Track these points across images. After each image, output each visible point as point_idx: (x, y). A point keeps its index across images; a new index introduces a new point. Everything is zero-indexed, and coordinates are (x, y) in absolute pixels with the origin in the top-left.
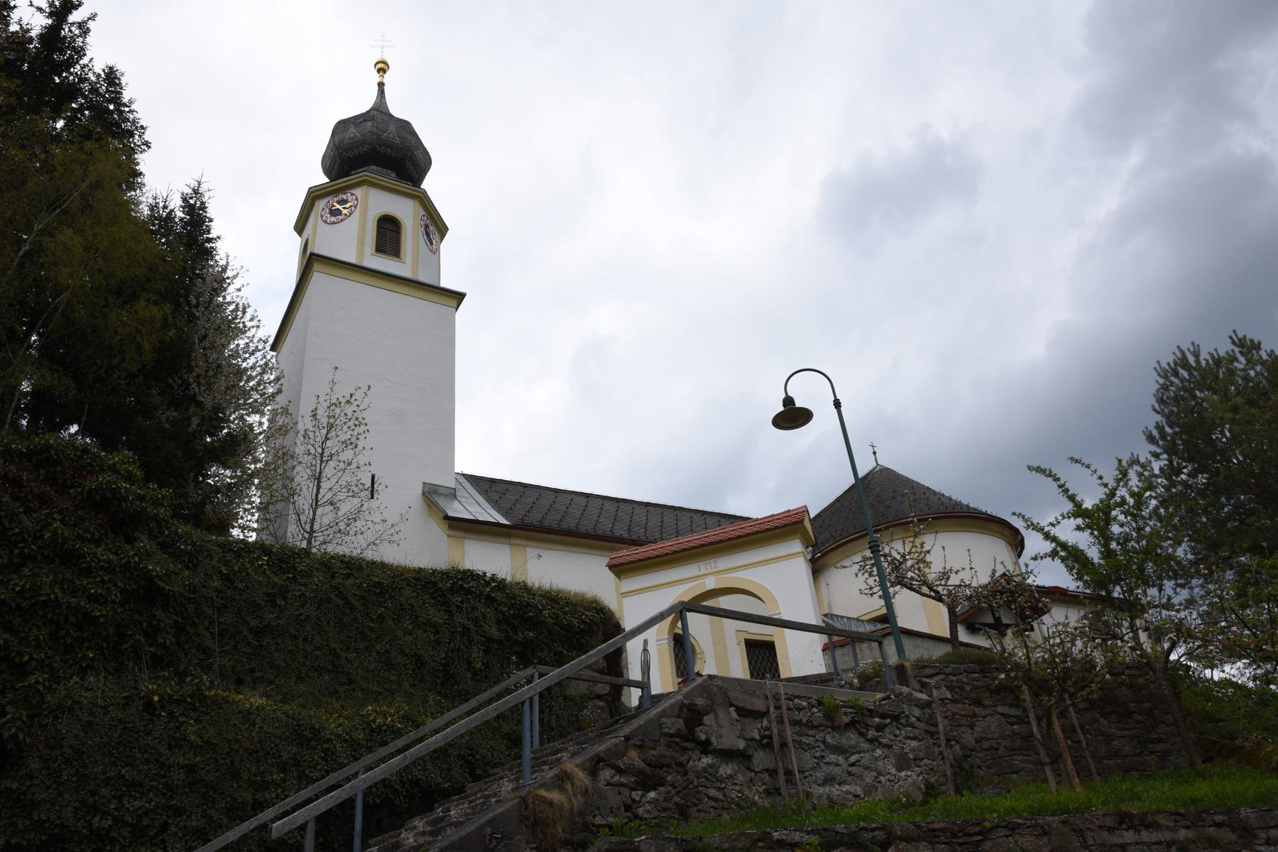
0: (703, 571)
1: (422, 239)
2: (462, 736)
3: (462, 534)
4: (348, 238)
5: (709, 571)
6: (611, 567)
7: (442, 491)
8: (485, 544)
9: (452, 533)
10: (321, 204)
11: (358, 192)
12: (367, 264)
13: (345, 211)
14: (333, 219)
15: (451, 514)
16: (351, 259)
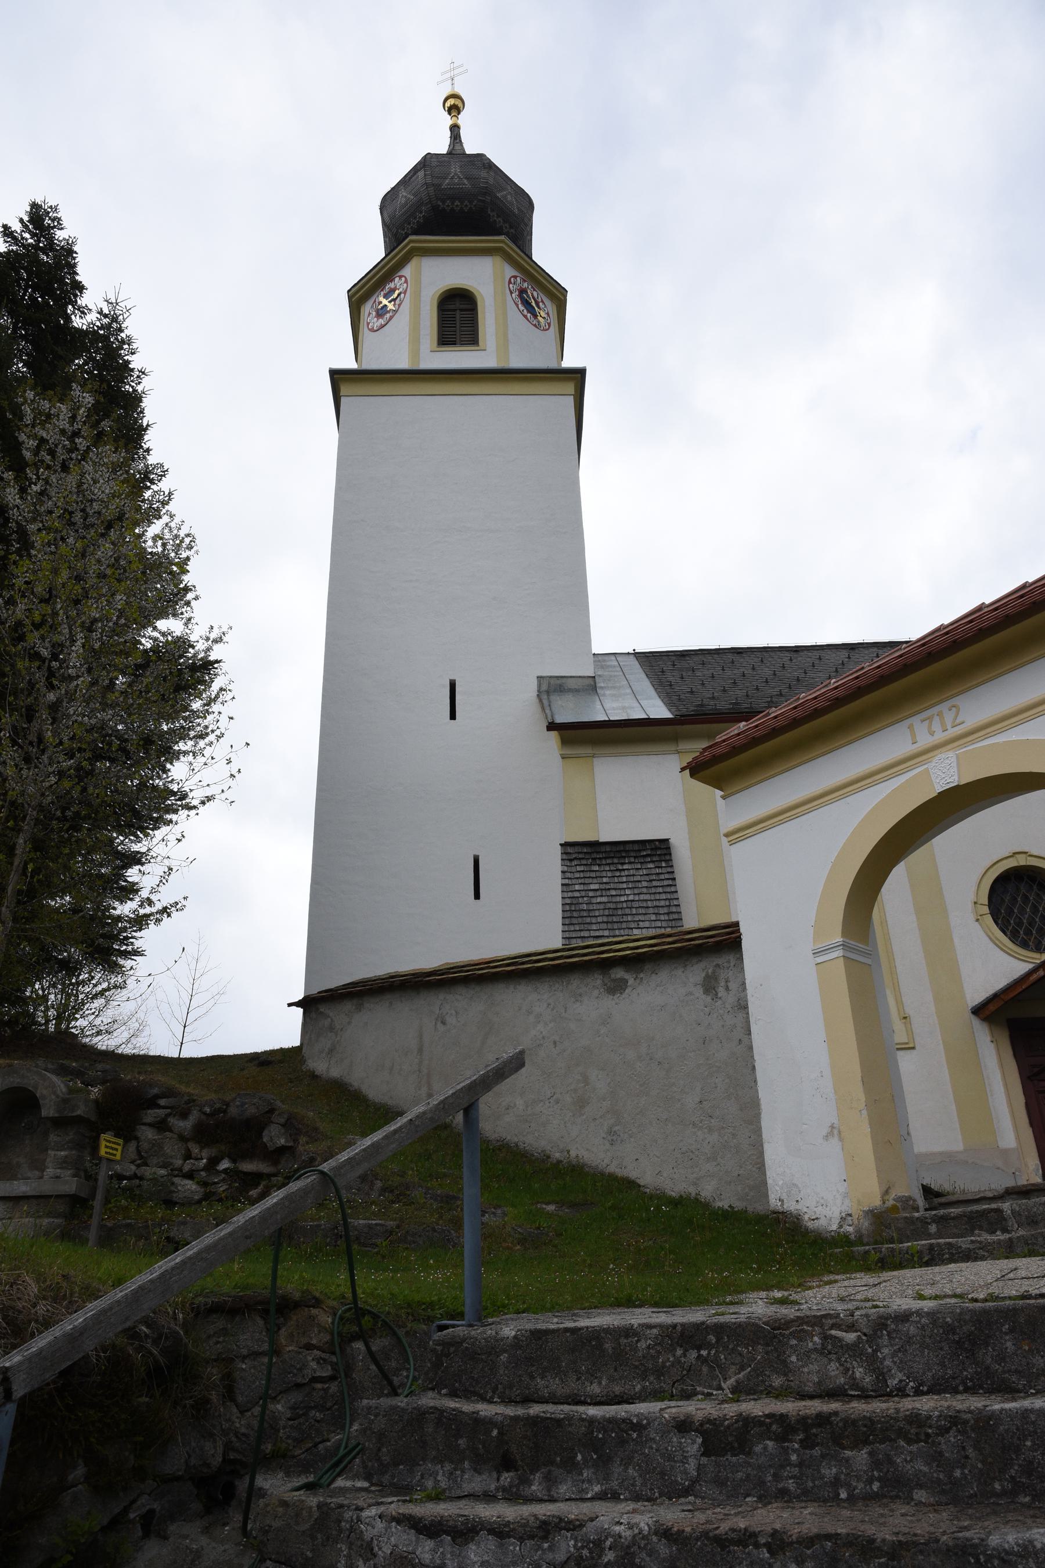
0: (925, 740)
1: (515, 314)
2: (48, 1384)
3: (588, 750)
4: (406, 337)
5: (940, 736)
6: (696, 769)
7: (571, 684)
8: (630, 760)
9: (568, 751)
10: (367, 308)
11: (407, 271)
12: (423, 366)
13: (391, 306)
14: (381, 321)
15: (560, 719)
16: (404, 364)
